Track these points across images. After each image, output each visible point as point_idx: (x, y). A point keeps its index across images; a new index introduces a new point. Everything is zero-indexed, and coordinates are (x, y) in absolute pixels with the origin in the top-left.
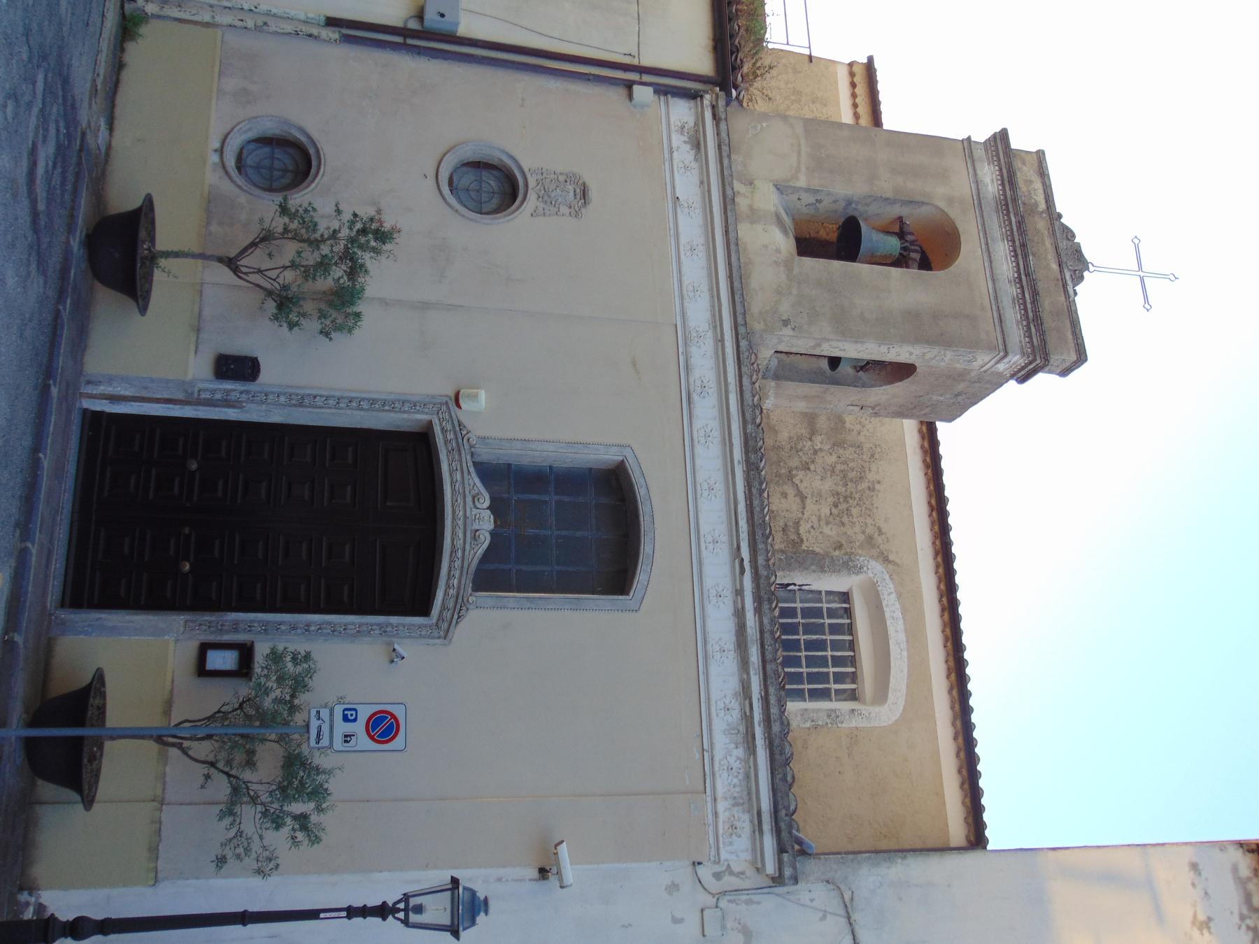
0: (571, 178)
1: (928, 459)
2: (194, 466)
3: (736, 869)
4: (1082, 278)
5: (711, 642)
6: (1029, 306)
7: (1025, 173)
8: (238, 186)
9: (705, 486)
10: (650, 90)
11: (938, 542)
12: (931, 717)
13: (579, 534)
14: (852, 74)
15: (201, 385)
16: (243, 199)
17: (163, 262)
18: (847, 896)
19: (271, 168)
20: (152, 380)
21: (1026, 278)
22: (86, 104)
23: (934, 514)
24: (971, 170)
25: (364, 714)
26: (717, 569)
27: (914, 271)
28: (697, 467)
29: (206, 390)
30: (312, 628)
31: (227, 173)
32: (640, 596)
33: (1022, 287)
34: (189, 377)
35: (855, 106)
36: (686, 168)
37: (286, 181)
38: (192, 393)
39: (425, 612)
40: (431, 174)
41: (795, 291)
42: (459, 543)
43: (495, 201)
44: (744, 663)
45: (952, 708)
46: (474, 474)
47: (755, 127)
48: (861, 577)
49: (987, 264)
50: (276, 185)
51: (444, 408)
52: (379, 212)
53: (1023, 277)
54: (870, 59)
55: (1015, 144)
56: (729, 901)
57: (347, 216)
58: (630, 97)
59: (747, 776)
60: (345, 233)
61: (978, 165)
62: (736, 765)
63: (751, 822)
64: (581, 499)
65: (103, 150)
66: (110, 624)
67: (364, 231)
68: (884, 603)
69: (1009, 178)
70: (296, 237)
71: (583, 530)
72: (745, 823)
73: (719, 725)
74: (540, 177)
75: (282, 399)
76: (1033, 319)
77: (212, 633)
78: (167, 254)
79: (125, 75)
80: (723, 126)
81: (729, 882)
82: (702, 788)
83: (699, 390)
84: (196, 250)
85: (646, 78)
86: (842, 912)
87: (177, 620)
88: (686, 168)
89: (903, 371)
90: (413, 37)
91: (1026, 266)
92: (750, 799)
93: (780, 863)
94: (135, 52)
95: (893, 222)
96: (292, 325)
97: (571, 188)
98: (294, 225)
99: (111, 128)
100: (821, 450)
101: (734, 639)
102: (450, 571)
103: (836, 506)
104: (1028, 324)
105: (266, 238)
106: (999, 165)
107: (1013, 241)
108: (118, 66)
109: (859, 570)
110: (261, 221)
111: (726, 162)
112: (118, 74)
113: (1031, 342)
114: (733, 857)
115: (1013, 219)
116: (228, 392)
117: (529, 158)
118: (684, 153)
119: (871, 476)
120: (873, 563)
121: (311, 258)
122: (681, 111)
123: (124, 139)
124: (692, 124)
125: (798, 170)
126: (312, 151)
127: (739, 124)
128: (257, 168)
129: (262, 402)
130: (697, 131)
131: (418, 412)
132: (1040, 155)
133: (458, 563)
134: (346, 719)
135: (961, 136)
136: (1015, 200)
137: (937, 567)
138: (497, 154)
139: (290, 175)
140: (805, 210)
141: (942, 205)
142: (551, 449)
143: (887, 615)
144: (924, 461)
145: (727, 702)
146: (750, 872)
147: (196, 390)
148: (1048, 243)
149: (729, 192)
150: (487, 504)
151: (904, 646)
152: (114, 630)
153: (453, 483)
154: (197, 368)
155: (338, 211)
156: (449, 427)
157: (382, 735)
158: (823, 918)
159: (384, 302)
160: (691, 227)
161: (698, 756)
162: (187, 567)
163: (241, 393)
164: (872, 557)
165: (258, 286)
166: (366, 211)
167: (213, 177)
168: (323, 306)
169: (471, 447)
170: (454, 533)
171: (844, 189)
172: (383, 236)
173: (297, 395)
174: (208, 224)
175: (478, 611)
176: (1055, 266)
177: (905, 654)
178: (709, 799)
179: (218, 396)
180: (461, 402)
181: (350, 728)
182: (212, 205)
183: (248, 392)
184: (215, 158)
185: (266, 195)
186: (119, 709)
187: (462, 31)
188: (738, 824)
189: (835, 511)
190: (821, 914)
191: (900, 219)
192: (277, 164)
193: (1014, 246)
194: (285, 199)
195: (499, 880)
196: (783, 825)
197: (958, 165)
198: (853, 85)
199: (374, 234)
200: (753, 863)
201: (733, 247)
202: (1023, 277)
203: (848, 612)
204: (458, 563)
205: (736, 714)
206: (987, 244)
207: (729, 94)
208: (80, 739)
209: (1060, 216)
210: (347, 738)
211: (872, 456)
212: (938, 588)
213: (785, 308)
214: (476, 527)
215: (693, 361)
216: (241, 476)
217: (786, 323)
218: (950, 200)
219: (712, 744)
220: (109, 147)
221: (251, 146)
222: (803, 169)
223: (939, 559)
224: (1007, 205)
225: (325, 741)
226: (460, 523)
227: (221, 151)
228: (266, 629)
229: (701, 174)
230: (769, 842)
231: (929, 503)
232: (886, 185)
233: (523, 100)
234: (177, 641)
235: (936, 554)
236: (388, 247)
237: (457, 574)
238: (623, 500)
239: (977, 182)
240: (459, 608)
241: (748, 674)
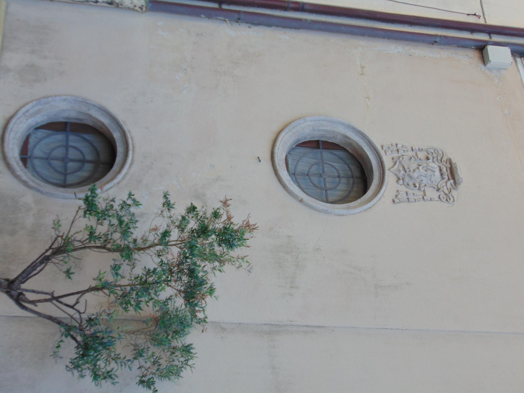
8: (25, 183)
10: (507, 51)
16: (28, 197)
19: (65, 160)
31: (8, 166)
37: (84, 174)
40: (266, 156)
50: (71, 179)
58: (484, 59)
67: (203, 231)
70: (105, 245)
74: (395, 155)
85: (496, 38)
97: (435, 166)
98: (102, 229)
105: (61, 249)
110: (57, 224)
117: (381, 131)
121: (130, 273)
126: (116, 135)
128: (47, 159)
138: (341, 130)
139: (88, 167)
155: (168, 205)
159: (221, 328)
165: (50, 318)
166: (207, 206)
168: (141, 340)
172: (229, 237)
185: (61, 191)
192: (73, 154)
194: (93, 191)
221: (41, 133)
233: (363, 67)
236: (236, 252)
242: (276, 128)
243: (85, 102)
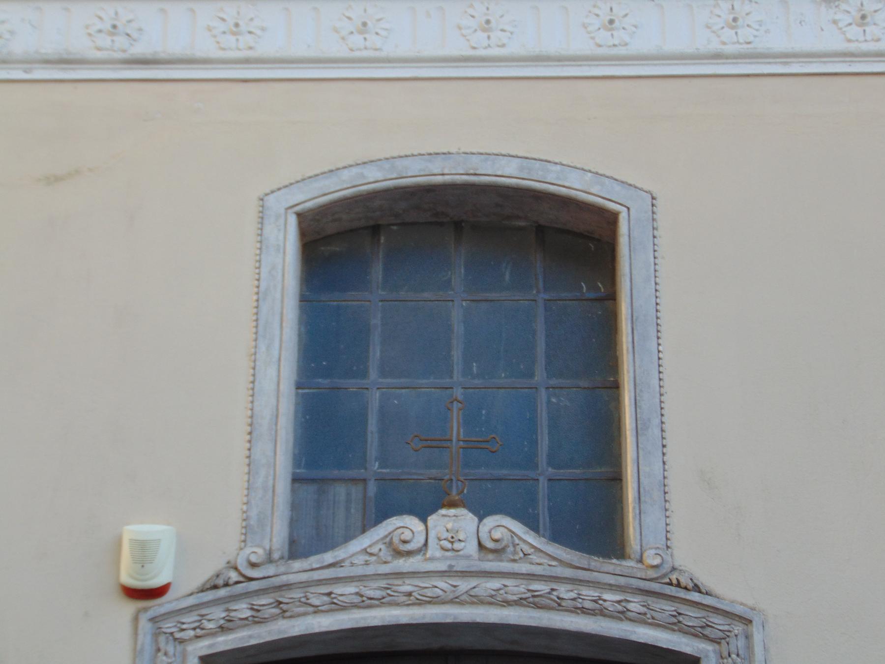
5: (715, 46)
9: (357, 40)
13: (459, 328)
28: (312, 53)
32: (617, 188)
42: (516, 588)
46: (340, 553)
51: (168, 626)
64: (376, 321)
102: (584, 611)
133: (565, 592)
142: (272, 372)
145: (845, 19)
150: (413, 523)
153: (365, 603)
156: (218, 613)
169: (270, 560)
170: (491, 601)
175: (674, 543)
204: (565, 592)
214: (471, 548)
215: (49, 48)
226: (464, 585)
237: (589, 593)
238: (375, 230)
240: (675, 590)
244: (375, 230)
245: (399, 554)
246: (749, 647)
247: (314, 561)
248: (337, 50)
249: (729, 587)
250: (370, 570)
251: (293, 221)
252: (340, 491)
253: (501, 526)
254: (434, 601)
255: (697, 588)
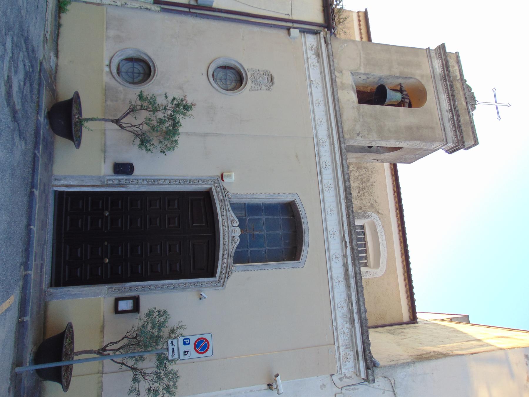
0: (266, 73)
1: (393, 172)
2: (107, 214)
3: (348, 375)
4: (475, 108)
5: (334, 278)
6: (456, 122)
7: (452, 62)
8: (119, 83)
9: (329, 210)
10: (298, 31)
11: (397, 205)
12: (395, 272)
13: (276, 232)
14: (359, 16)
15: (108, 178)
16: (121, 88)
17: (85, 124)
18: (393, 383)
19: (133, 73)
20: (85, 177)
21: (454, 110)
22: (41, 48)
23: (396, 194)
24: (430, 62)
25: (193, 340)
26: (335, 246)
27: (407, 109)
28: (325, 201)
29: (110, 180)
30: (165, 287)
31: (113, 76)
33: (452, 114)
34: (102, 174)
35: (360, 29)
36: (314, 66)
37: (140, 78)
38: (104, 182)
39: (212, 274)
41: (361, 120)
43: (233, 84)
44: (348, 287)
45: (403, 268)
47: (341, 46)
48: (369, 220)
49: (438, 104)
50: (136, 80)
51: (217, 182)
52: (185, 96)
53: (453, 109)
54: (366, 10)
55: (448, 50)
56: (346, 390)
57: (170, 98)
58: (289, 34)
59: (351, 336)
60: (170, 106)
61: (433, 60)
62: (347, 331)
63: (354, 355)
65: (54, 68)
66: (73, 293)
67: (178, 105)
68: (378, 229)
69: (446, 66)
71: (279, 232)
72: (351, 356)
73: (339, 314)
74: (252, 73)
75: (145, 182)
76: (458, 128)
77: (120, 293)
78: (87, 120)
79: (62, 29)
80: (329, 46)
81: (346, 381)
82: (333, 342)
83: (324, 166)
84: (101, 117)
85: (295, 25)
86: (391, 390)
87: (104, 288)
88: (314, 66)
89: (399, 148)
90: (193, 8)
91: (454, 104)
92: (353, 345)
93: (367, 373)
94: (65, 18)
95: (397, 85)
96: (148, 150)
97: (266, 77)
99: (57, 56)
100: (353, 170)
101: (343, 276)
102: (223, 256)
103: (359, 192)
104: (456, 130)
105: (132, 110)
106: (442, 60)
107: (448, 93)
108: (58, 26)
109: (368, 217)
110: (130, 102)
111: (332, 63)
112: (59, 29)
113: (457, 137)
114: (347, 371)
115: (448, 84)
116: (120, 180)
117: (248, 64)
118: (313, 60)
119: (372, 180)
120: (373, 214)
122: (311, 40)
123: (64, 60)
124: (315, 46)
125: (360, 65)
126: (151, 64)
127: (335, 45)
129: (135, 184)
130: (318, 49)
131: (205, 184)
132: (457, 54)
133: (226, 252)
134: (185, 344)
135: (425, 47)
136: (449, 75)
137: (397, 214)
138: (233, 63)
139: (142, 76)
140: (361, 82)
141: (419, 78)
142: (264, 197)
143: (379, 234)
144: (391, 173)
146: (354, 376)
147: (106, 180)
148: (461, 93)
149: (334, 77)
151: (385, 246)
152: (76, 296)
153: (222, 216)
154: (106, 170)
156: (219, 190)
157: (202, 350)
158: (384, 393)
159: (187, 134)
160: (317, 93)
161: (331, 328)
162: (107, 261)
163: (126, 180)
164: (373, 212)
167: (107, 79)
171: (380, 73)
172: (188, 108)
173: (152, 179)
174: (106, 101)
175: (236, 273)
176: (464, 103)
177: (386, 249)
178: (336, 347)
179: (116, 182)
180: (224, 179)
181: (186, 348)
182: (107, 91)
183: (129, 180)
184: (107, 69)
185: (132, 86)
186: (81, 343)
187: (215, 5)
188: (348, 357)
189: (358, 194)
190: (383, 391)
191: (400, 84)
192: (136, 70)
193: (449, 95)
195: (251, 391)
196: (368, 358)
197: (425, 61)
198: (359, 21)
199: (183, 107)
200: (355, 373)
201: (336, 102)
202: (453, 109)
203: (364, 233)
204: (226, 252)
205: (346, 309)
206: (438, 95)
207: (331, 32)
208: (60, 367)
209: (466, 81)
210: (186, 353)
211: (372, 172)
212: (398, 222)
213: (358, 128)
215: (321, 154)
216: (129, 217)
217: (358, 134)
218: (422, 76)
219: (336, 323)
220: (57, 66)
222: (362, 64)
223: (398, 212)
224: (445, 77)
225: (176, 356)
226: (226, 234)
227: (109, 66)
228: (144, 288)
229: (321, 68)
230: (362, 364)
231: (394, 190)
232: (396, 71)
233: (243, 37)
234: (104, 297)
235: (397, 209)
237: (226, 257)
238: (293, 216)
239: (433, 68)
240: (228, 273)
241: (350, 291)
242: (209, 62)
243: (139, 51)
244: (293, 216)
245: (232, 222)
246: (218, 287)
247: (229, 206)
248: (327, 206)
249: (229, 283)
250: (228, 216)
251: (293, 199)
252: (243, 212)
253: (238, 240)
254: (223, 229)
255: (228, 276)
